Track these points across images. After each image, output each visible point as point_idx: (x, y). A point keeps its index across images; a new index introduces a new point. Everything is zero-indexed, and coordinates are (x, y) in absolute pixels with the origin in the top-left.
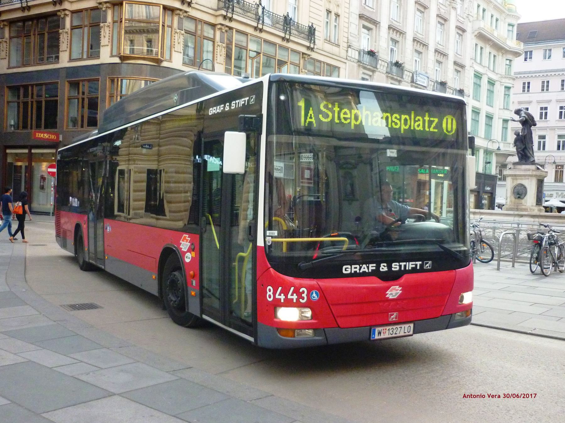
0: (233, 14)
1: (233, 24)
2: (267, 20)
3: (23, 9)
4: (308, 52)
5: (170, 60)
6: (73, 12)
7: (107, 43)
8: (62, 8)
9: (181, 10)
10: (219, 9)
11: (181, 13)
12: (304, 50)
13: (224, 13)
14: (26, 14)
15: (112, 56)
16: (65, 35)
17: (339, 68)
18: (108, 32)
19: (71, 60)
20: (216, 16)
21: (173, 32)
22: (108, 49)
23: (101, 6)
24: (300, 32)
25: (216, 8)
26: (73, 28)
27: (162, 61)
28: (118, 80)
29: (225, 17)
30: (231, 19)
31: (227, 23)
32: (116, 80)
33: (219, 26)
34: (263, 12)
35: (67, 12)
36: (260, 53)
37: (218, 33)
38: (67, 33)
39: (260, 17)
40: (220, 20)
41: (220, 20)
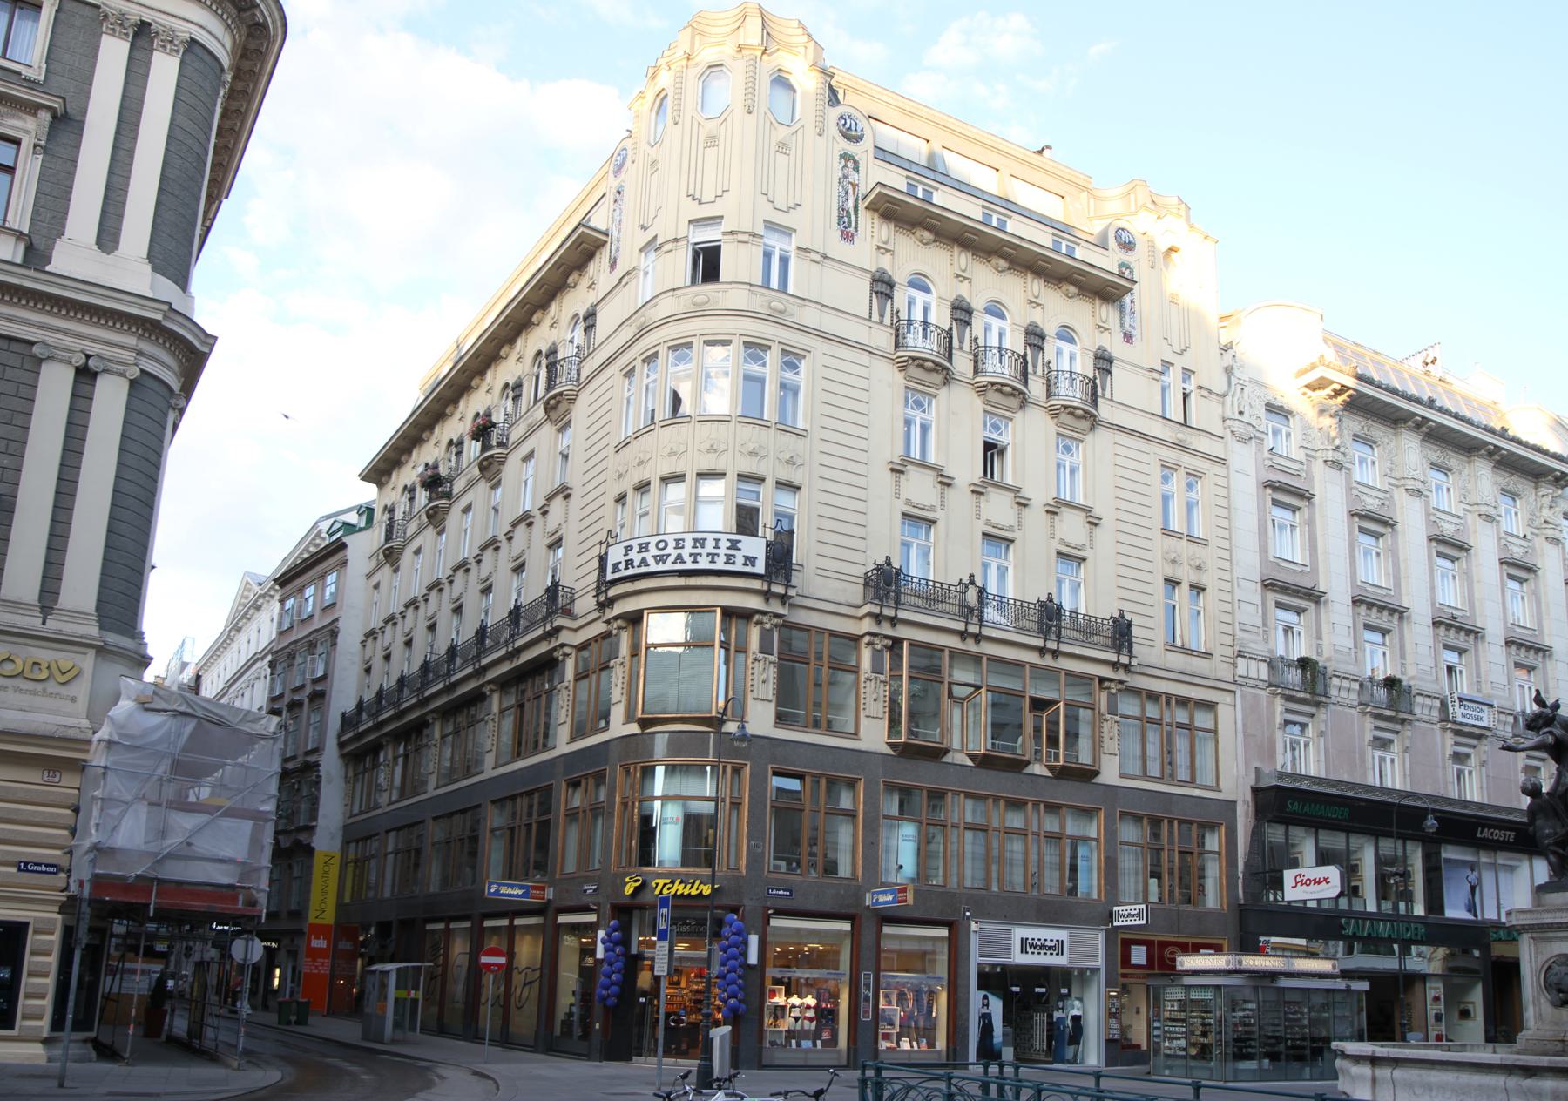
35: (567, 650)
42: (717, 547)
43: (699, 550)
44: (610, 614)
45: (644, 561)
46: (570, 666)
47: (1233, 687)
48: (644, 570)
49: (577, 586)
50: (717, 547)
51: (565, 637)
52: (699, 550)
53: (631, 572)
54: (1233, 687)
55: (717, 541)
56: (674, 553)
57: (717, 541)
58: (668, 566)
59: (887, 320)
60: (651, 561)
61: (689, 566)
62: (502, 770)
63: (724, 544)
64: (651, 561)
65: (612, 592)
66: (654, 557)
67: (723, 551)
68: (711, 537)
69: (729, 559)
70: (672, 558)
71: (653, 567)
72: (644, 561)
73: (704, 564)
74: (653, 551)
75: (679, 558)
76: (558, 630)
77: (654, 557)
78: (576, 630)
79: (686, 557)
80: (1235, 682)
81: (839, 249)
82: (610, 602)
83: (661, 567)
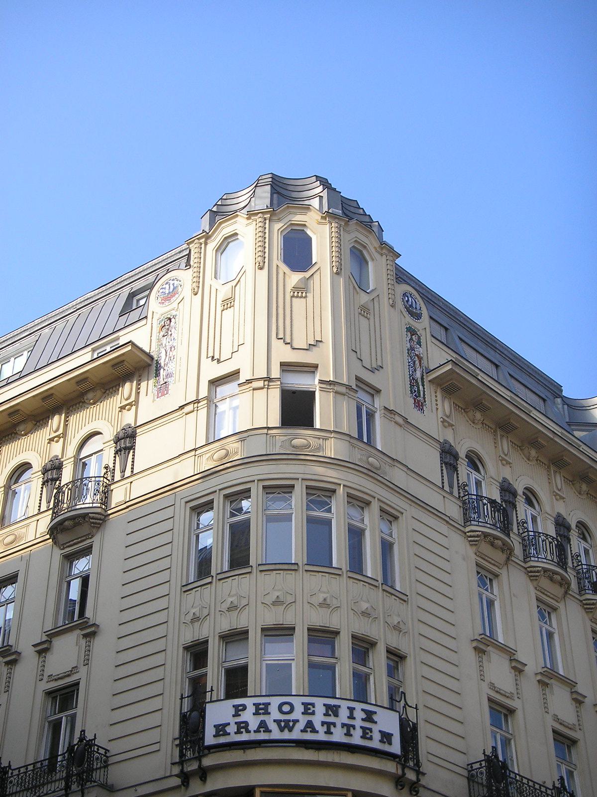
42: (351, 717)
43: (331, 719)
45: (263, 726)
48: (263, 736)
49: (114, 748)
50: (351, 717)
52: (331, 719)
53: (244, 737)
55: (351, 710)
56: (303, 721)
57: (351, 710)
58: (296, 734)
59: (456, 494)
60: (273, 726)
61: (321, 736)
63: (359, 715)
64: (273, 726)
65: (207, 762)
66: (277, 722)
67: (358, 723)
68: (344, 705)
69: (366, 733)
70: (301, 725)
71: (276, 734)
72: (263, 726)
73: (338, 736)
74: (275, 714)
75: (310, 726)
77: (277, 722)
79: (318, 726)
81: (414, 416)
82: (203, 774)
83: (286, 735)
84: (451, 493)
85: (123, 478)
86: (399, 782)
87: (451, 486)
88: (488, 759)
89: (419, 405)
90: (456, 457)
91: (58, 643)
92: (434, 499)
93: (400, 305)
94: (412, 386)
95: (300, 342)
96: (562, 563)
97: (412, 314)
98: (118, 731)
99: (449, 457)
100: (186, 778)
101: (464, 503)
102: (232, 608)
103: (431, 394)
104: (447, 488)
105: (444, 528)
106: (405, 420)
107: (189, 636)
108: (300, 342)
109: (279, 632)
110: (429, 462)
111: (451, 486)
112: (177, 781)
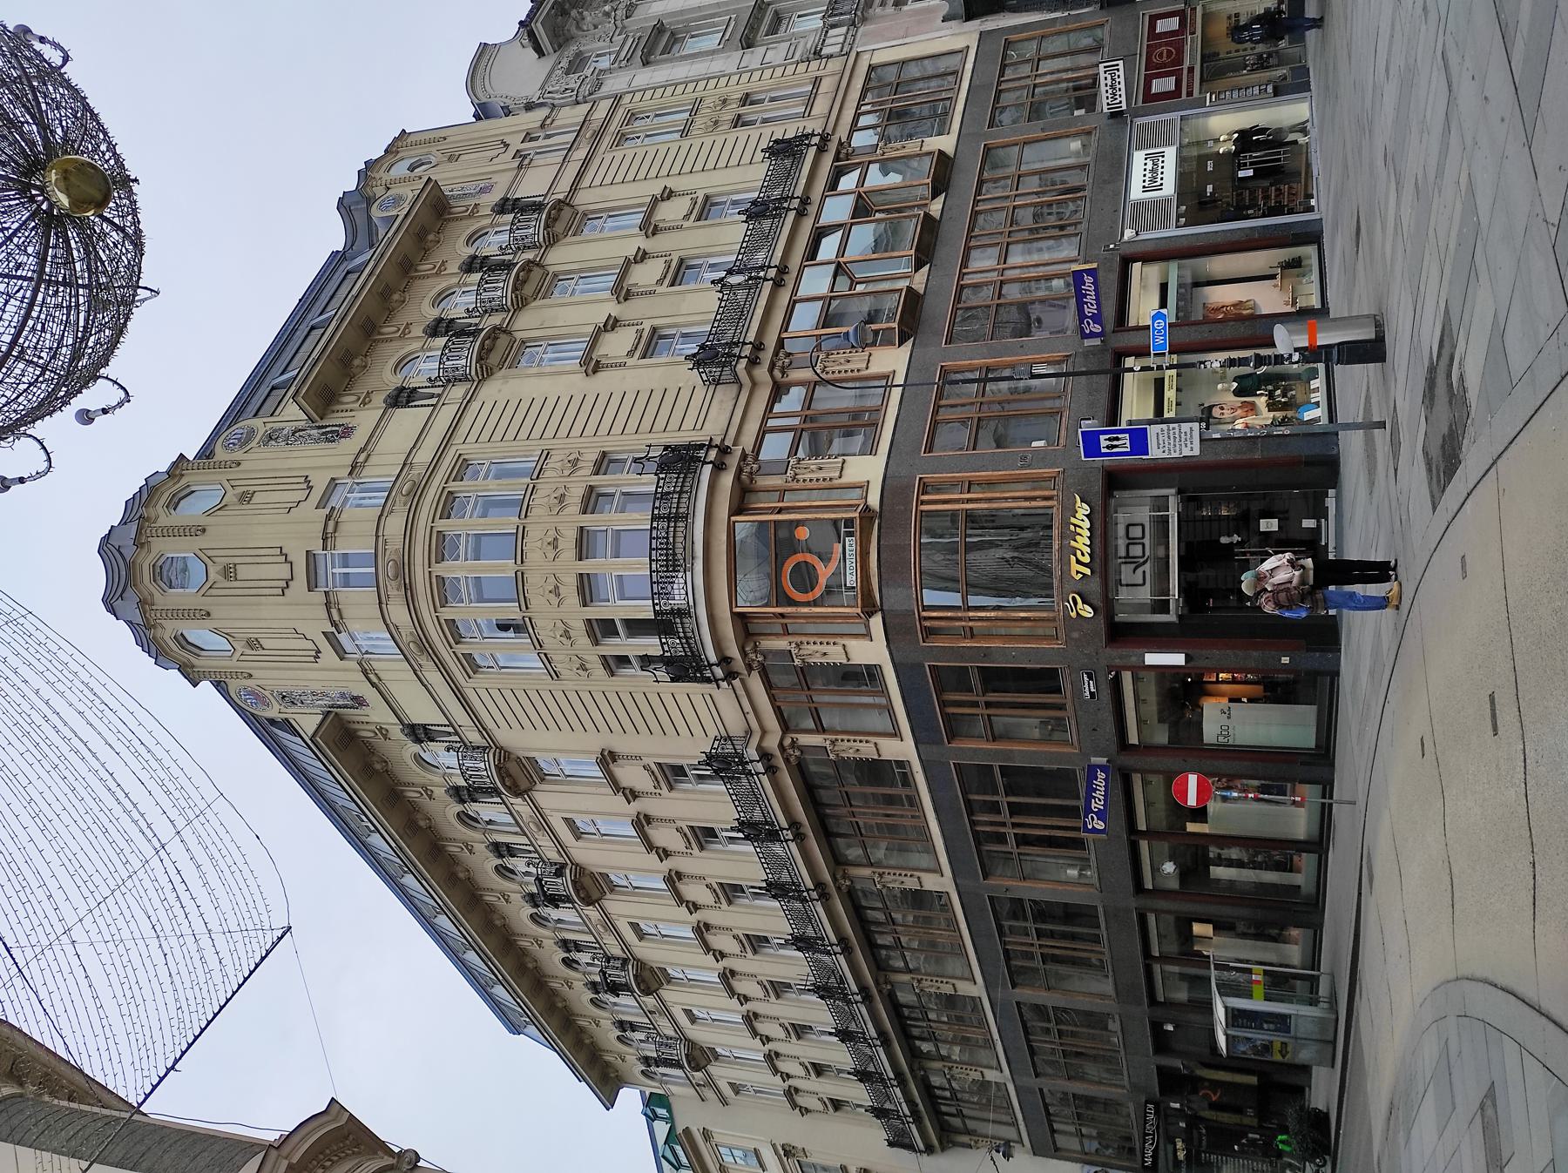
0: (744, 343)
1: (771, 341)
2: (760, 257)
3: (799, 837)
4: (833, 147)
5: (864, 487)
6: (786, 727)
7: (840, 648)
8: (778, 753)
9: (740, 470)
10: (737, 381)
11: (747, 469)
12: (828, 161)
13: (744, 362)
14: (807, 829)
15: (868, 635)
16: (840, 746)
17: (872, 68)
18: (812, 648)
19: (896, 734)
20: (754, 384)
21: (794, 485)
22: (852, 644)
23: (755, 665)
24: (789, 175)
25: (735, 387)
26: (821, 729)
27: (867, 508)
28: (926, 619)
29: (753, 362)
30: (758, 346)
31: (766, 356)
32: (927, 624)
33: (777, 373)
34: (740, 272)
35: (787, 742)
36: (839, 265)
37: (795, 375)
38: (833, 742)
39: (750, 278)
40: (762, 373)
41: (762, 373)
44: (739, 664)
46: (805, 740)
47: (853, 55)
49: (713, 733)
51: (772, 743)
54: (853, 55)
62: (944, 860)
76: (765, 756)
78: (764, 732)
80: (848, 54)
82: (724, 660)
84: (439, 396)
85: (457, 733)
86: (719, 467)
87: (432, 396)
88: (697, 365)
89: (347, 432)
90: (401, 389)
91: (624, 783)
92: (446, 415)
93: (238, 455)
94: (328, 440)
95: (284, 571)
96: (508, 266)
97: (249, 439)
98: (697, 730)
99: (402, 398)
100: (730, 675)
101: (449, 381)
102: (567, 635)
103: (334, 420)
104: (434, 401)
105: (475, 406)
106: (362, 450)
107: (599, 671)
108: (284, 571)
109: (587, 589)
110: (408, 420)
111: (432, 396)
112: (737, 682)
